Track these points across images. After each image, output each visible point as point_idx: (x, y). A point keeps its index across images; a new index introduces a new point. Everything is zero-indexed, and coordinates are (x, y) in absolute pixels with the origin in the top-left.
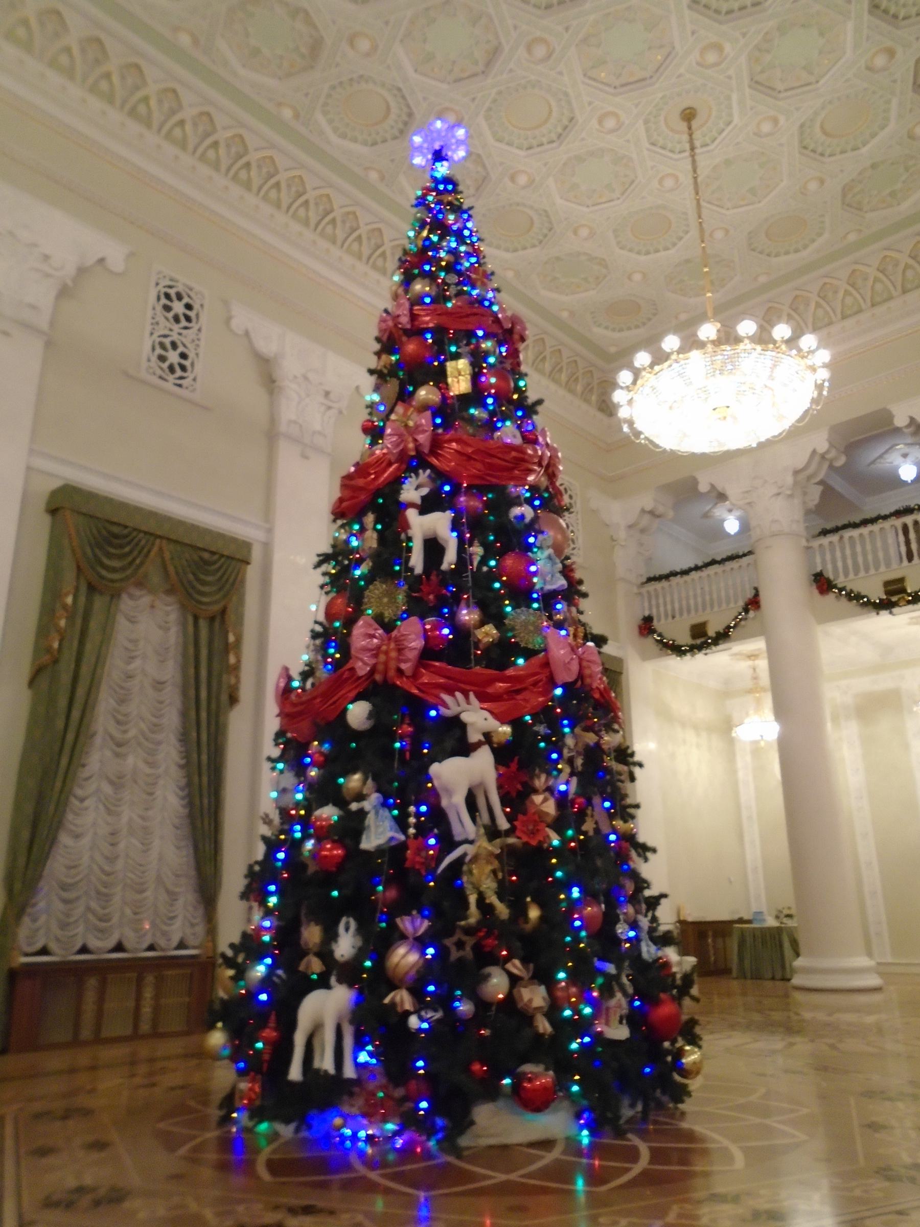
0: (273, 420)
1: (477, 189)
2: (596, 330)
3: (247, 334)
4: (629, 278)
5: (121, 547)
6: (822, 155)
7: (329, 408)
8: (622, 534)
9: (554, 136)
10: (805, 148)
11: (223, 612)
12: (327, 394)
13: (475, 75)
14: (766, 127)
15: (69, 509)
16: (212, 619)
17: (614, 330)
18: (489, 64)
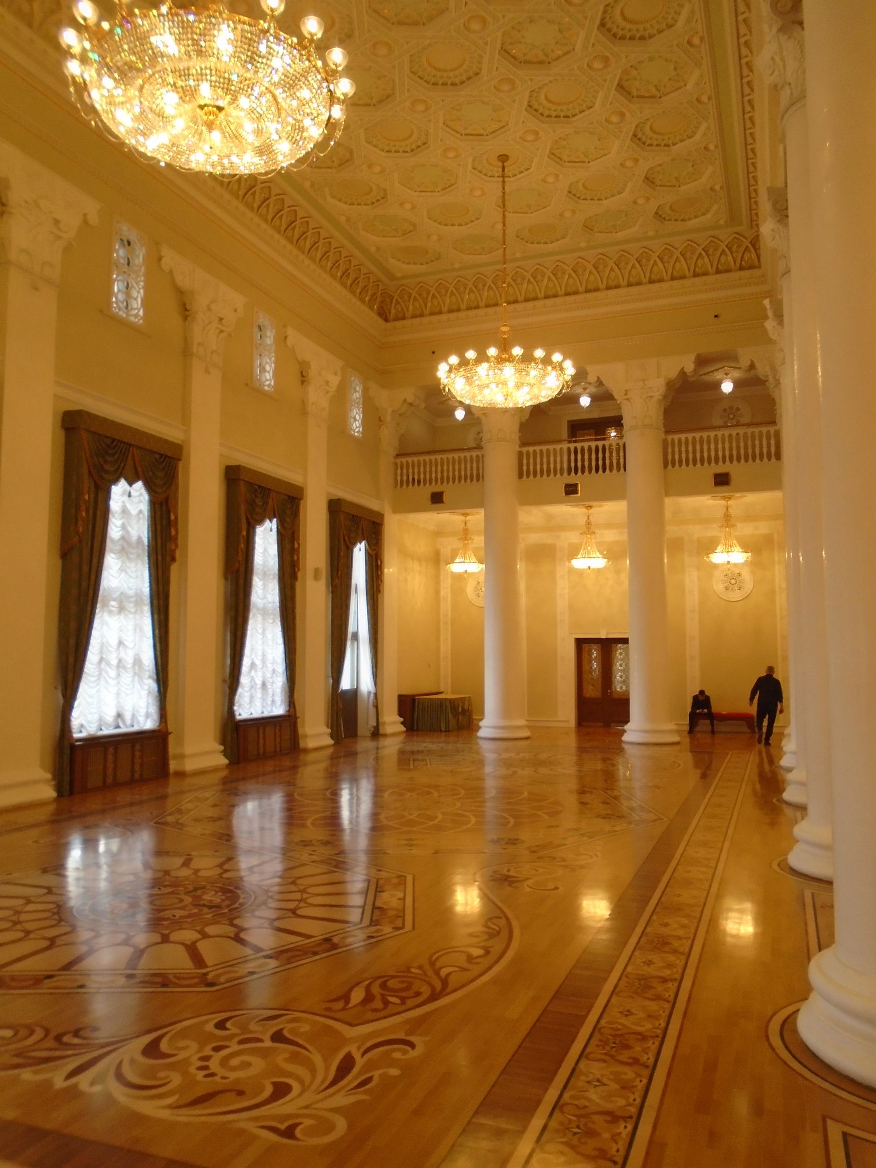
0: (187, 341)
1: (340, 165)
2: (392, 261)
3: (171, 272)
4: (429, 237)
5: (114, 455)
6: (579, 198)
7: (222, 331)
8: (388, 418)
9: (408, 149)
10: (570, 192)
11: (167, 499)
12: (221, 319)
13: (369, 105)
14: (551, 179)
15: (73, 424)
16: (161, 504)
17: (403, 262)
18: (381, 101)
